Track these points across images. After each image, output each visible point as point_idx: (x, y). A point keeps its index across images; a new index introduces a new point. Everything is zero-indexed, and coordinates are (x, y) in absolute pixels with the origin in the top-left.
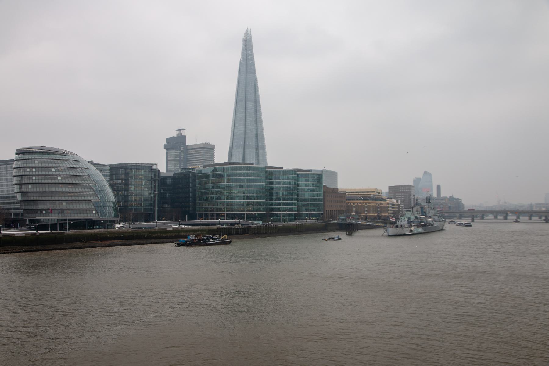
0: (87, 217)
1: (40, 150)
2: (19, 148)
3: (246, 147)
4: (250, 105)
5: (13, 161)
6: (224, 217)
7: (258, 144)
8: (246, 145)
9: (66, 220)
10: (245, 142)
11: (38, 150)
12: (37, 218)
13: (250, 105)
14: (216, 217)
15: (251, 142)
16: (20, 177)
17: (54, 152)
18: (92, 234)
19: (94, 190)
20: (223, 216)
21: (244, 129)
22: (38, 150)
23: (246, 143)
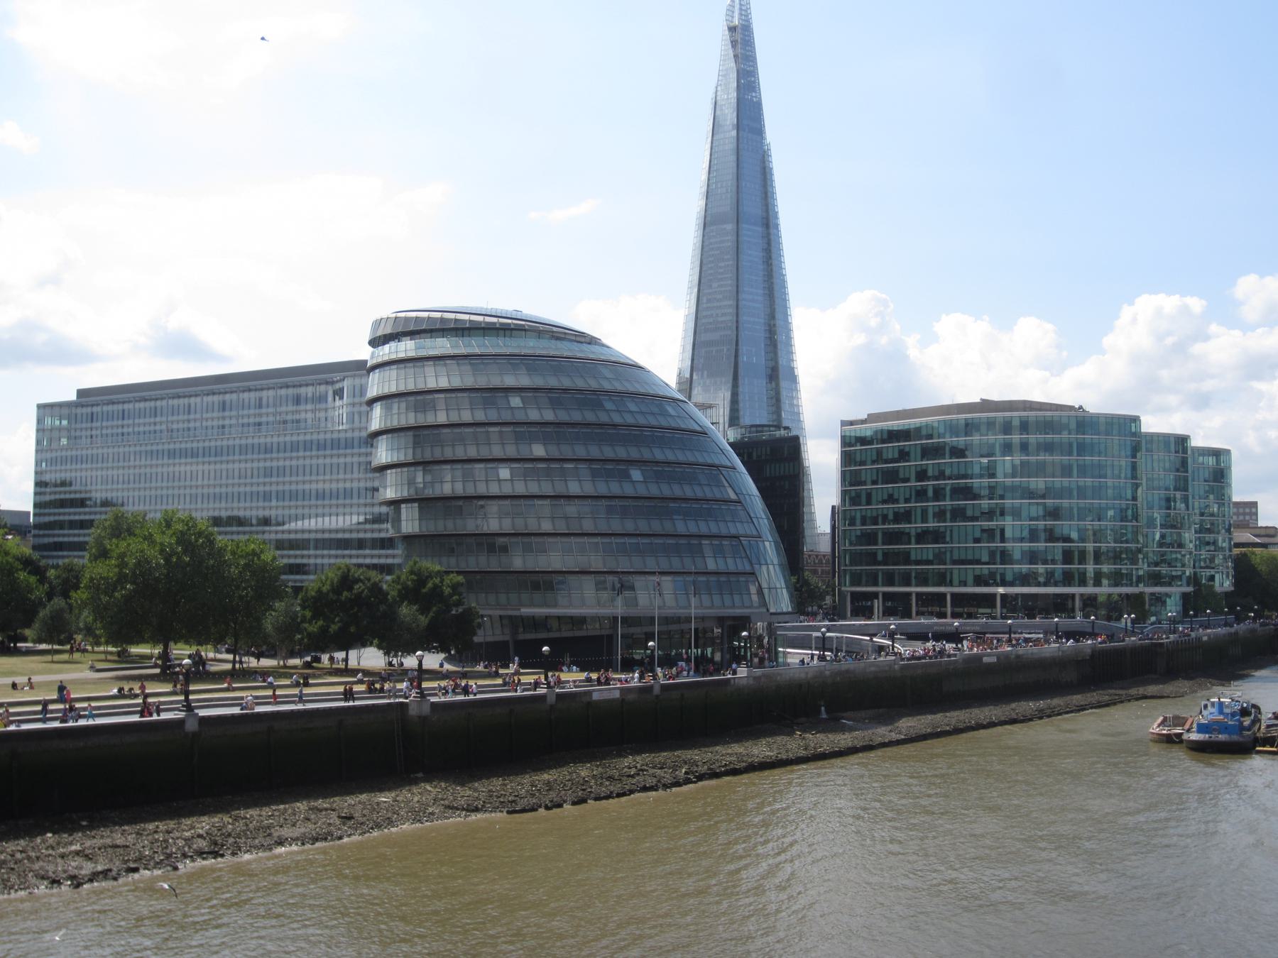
0: (733, 606)
1: (502, 320)
2: (387, 311)
3: (741, 372)
4: (752, 233)
5: (359, 368)
6: (993, 606)
7: (777, 362)
8: (741, 365)
9: (688, 620)
10: (736, 356)
11: (495, 320)
12: (526, 611)
13: (752, 233)
14: (952, 606)
15: (753, 355)
16: (411, 433)
17: (555, 329)
18: (800, 686)
19: (736, 494)
20: (989, 600)
21: (732, 310)
22: (495, 320)
23: (740, 359)
